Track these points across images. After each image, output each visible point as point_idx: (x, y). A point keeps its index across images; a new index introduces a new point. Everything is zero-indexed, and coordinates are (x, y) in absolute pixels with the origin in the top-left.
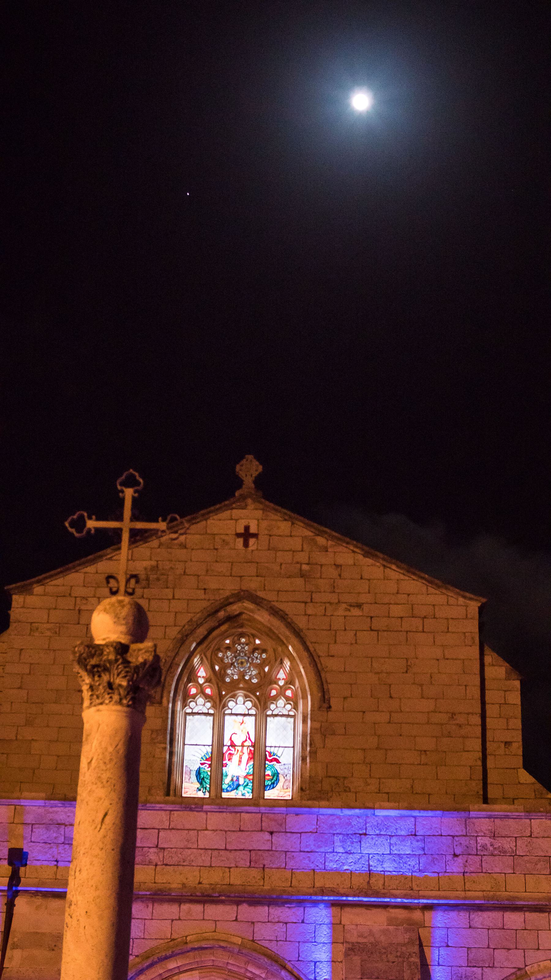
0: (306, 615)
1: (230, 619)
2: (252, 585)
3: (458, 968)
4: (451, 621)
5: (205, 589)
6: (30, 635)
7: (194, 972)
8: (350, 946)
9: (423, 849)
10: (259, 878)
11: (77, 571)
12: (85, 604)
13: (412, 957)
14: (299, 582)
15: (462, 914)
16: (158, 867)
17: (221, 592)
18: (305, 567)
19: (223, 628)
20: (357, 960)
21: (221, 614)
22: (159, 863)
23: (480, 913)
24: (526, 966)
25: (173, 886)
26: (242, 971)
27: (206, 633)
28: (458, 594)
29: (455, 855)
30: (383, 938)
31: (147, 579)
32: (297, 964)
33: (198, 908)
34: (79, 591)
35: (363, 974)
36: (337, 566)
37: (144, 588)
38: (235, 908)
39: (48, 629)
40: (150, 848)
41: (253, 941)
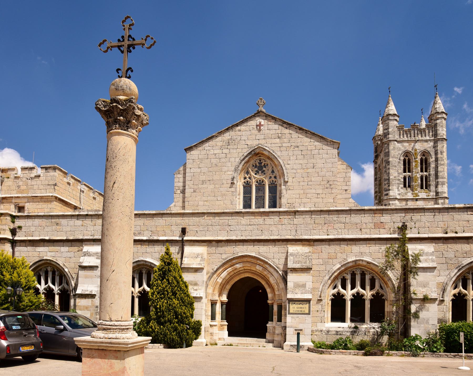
9: (314, 222)
13: (310, 256)
14: (278, 140)
15: (327, 242)
23: (332, 242)
26: (256, 263)
29: (325, 224)
30: (300, 251)
31: (229, 143)
35: (294, 262)
37: (228, 145)
38: (253, 243)
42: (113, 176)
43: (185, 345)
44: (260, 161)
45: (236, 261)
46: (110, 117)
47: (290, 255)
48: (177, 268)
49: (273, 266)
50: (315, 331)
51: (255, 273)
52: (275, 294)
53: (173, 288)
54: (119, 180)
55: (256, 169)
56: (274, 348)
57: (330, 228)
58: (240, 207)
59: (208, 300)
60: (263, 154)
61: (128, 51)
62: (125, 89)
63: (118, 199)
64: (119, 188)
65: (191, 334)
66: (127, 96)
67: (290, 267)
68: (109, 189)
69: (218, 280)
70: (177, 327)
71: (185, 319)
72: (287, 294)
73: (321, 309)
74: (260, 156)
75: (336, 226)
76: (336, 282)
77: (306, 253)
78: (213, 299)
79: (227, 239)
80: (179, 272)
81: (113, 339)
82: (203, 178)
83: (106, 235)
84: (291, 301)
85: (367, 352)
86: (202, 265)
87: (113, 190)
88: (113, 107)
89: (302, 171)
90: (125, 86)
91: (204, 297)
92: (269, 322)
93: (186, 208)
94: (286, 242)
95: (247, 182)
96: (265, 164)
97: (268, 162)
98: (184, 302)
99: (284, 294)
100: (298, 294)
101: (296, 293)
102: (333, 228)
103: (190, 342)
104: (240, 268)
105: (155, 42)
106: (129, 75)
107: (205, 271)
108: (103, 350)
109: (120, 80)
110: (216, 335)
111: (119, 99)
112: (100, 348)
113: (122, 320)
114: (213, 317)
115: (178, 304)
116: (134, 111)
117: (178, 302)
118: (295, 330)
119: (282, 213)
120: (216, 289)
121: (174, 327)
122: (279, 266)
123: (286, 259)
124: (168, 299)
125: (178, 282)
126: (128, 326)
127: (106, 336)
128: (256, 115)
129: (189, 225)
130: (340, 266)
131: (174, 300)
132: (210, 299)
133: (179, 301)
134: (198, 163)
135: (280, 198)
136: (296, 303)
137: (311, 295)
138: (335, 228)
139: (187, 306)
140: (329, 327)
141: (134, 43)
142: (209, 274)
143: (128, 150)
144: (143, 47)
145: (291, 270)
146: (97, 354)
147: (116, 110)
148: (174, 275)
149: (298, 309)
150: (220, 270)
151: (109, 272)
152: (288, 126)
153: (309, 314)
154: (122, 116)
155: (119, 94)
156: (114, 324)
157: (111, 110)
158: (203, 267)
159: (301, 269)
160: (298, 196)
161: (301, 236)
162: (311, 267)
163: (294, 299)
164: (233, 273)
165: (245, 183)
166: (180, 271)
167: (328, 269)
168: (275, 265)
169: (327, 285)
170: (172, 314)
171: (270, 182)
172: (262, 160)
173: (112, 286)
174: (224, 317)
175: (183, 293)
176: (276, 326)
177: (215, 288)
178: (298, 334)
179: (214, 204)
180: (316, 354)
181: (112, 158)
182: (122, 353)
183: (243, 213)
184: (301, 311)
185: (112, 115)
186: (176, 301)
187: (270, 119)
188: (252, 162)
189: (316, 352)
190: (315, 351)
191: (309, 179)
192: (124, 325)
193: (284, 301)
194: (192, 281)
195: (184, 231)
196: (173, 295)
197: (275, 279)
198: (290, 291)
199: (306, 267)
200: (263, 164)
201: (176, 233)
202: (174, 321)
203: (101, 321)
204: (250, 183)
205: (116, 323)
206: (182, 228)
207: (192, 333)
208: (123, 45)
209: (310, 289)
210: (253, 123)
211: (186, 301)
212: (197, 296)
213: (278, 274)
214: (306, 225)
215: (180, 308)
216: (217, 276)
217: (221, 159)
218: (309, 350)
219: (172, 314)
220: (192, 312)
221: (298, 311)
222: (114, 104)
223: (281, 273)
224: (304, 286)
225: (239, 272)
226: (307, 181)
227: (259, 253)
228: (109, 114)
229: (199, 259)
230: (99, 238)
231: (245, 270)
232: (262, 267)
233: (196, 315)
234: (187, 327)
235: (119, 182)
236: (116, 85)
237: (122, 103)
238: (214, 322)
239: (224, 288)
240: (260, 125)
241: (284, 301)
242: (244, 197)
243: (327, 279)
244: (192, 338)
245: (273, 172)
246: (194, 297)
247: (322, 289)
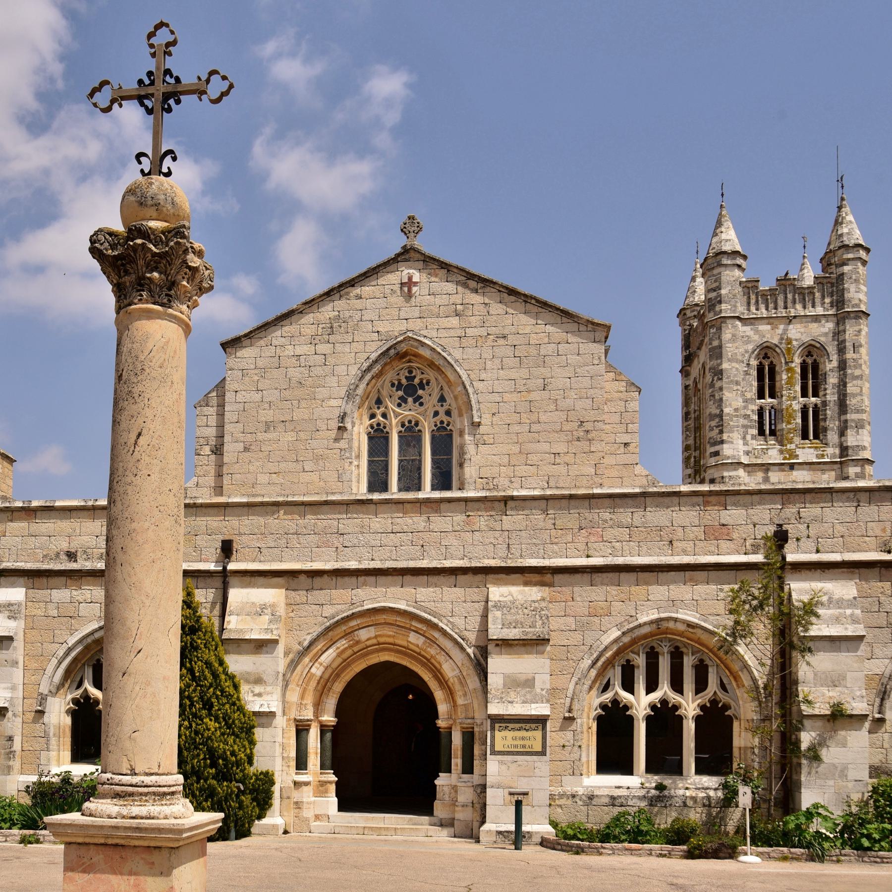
7: (370, 628)
13: (543, 610)
26: (408, 626)
30: (520, 597)
31: (332, 327)
35: (503, 625)
38: (401, 577)
42: (135, 417)
43: (233, 834)
44: (410, 372)
45: (359, 622)
46: (127, 273)
47: (495, 606)
48: (213, 640)
49: (450, 635)
50: (557, 797)
51: (405, 651)
52: (455, 705)
53: (203, 691)
54: (152, 427)
55: (400, 393)
56: (456, 839)
57: (592, 539)
58: (361, 490)
59: (289, 720)
60: (416, 355)
61: (163, 109)
62: (162, 203)
63: (149, 475)
64: (151, 446)
65: (247, 807)
66: (166, 221)
67: (495, 637)
68: (125, 451)
69: (313, 670)
70: (215, 789)
71: (235, 768)
72: (488, 704)
73: (572, 741)
74: (409, 361)
75: (609, 534)
76: (610, 674)
77: (534, 602)
78: (302, 718)
79: (336, 567)
80: (216, 649)
81: (142, 818)
82: (267, 415)
83: (119, 563)
84: (498, 720)
85: (695, 848)
86: (274, 632)
87: (136, 452)
88: (135, 248)
89: (515, 397)
90: (163, 197)
91: (279, 713)
92: (440, 774)
93: (224, 492)
94: (484, 576)
95: (379, 425)
96: (421, 380)
97: (431, 375)
98: (231, 725)
99: (479, 705)
100: (514, 705)
101: (509, 702)
102: (600, 539)
103: (247, 826)
104: (368, 640)
105: (231, 86)
106: (169, 168)
107: (280, 649)
108: (116, 845)
109: (149, 180)
110: (308, 806)
111: (150, 228)
112: (110, 841)
113: (160, 772)
114: (301, 764)
115: (216, 731)
116: (185, 257)
117: (217, 725)
118: (511, 794)
119: (473, 503)
120: (307, 692)
121: (208, 788)
122: (466, 633)
123: (485, 616)
124: (193, 718)
125: (215, 676)
126: (174, 786)
127: (124, 811)
128: (399, 259)
129: (240, 534)
130: (619, 633)
131: (207, 720)
132: (292, 717)
133: (219, 723)
135: (461, 465)
136: (511, 726)
138: (605, 539)
139: (237, 736)
140: (592, 787)
141: (179, 90)
142: (291, 656)
143: (172, 354)
144: (201, 100)
145: (497, 645)
146: (102, 856)
147: (142, 257)
148: (206, 657)
149: (515, 743)
150: (319, 646)
151: (128, 654)
152: (480, 285)
153: (543, 753)
154: (155, 269)
155: (148, 216)
156: (143, 782)
157: (131, 256)
158: (277, 638)
159: (521, 642)
160: (505, 460)
161: (520, 560)
162: (547, 637)
163: (505, 717)
164: (349, 652)
165: (372, 427)
166: (220, 648)
167: (589, 641)
168: (457, 631)
169: (586, 682)
170: (202, 756)
171: (436, 426)
172: (414, 371)
173: (137, 688)
174: (328, 762)
175: (228, 703)
176: (459, 784)
177: (305, 690)
178: (518, 805)
179: (297, 481)
180: (564, 853)
181: (132, 373)
182: (165, 853)
183: (376, 504)
184: (524, 746)
185: (132, 268)
186: (213, 723)
187: (435, 267)
188: (390, 376)
189: (564, 848)
190: (559, 847)
191: (534, 417)
192: (165, 784)
193: (479, 722)
194: (248, 673)
195: (227, 549)
196: (204, 708)
197: (455, 667)
198: (495, 697)
199: (534, 637)
200: (417, 381)
201: (207, 553)
202: (208, 772)
203: (109, 775)
204: (385, 427)
205: (148, 780)
206: (223, 542)
207: (251, 804)
208: (152, 95)
209: (544, 692)
210: (392, 279)
211: (237, 722)
212: (261, 710)
213: (464, 655)
215: (221, 741)
218: (544, 843)
219: (202, 756)
220: (251, 749)
221: (516, 746)
222: (139, 241)
223: (470, 651)
224: (529, 683)
225: (364, 649)
226: (528, 421)
227: (416, 602)
228: (123, 265)
230: (13, 567)
231: (379, 644)
232: (424, 636)
233: (260, 759)
234: (238, 788)
235: (151, 432)
236: (139, 194)
237: (155, 239)
238: (302, 774)
240: (409, 284)
241: (479, 722)
242: (370, 463)
243: (587, 666)
244: (252, 816)
245: (442, 399)
246: (255, 714)
247: (574, 692)
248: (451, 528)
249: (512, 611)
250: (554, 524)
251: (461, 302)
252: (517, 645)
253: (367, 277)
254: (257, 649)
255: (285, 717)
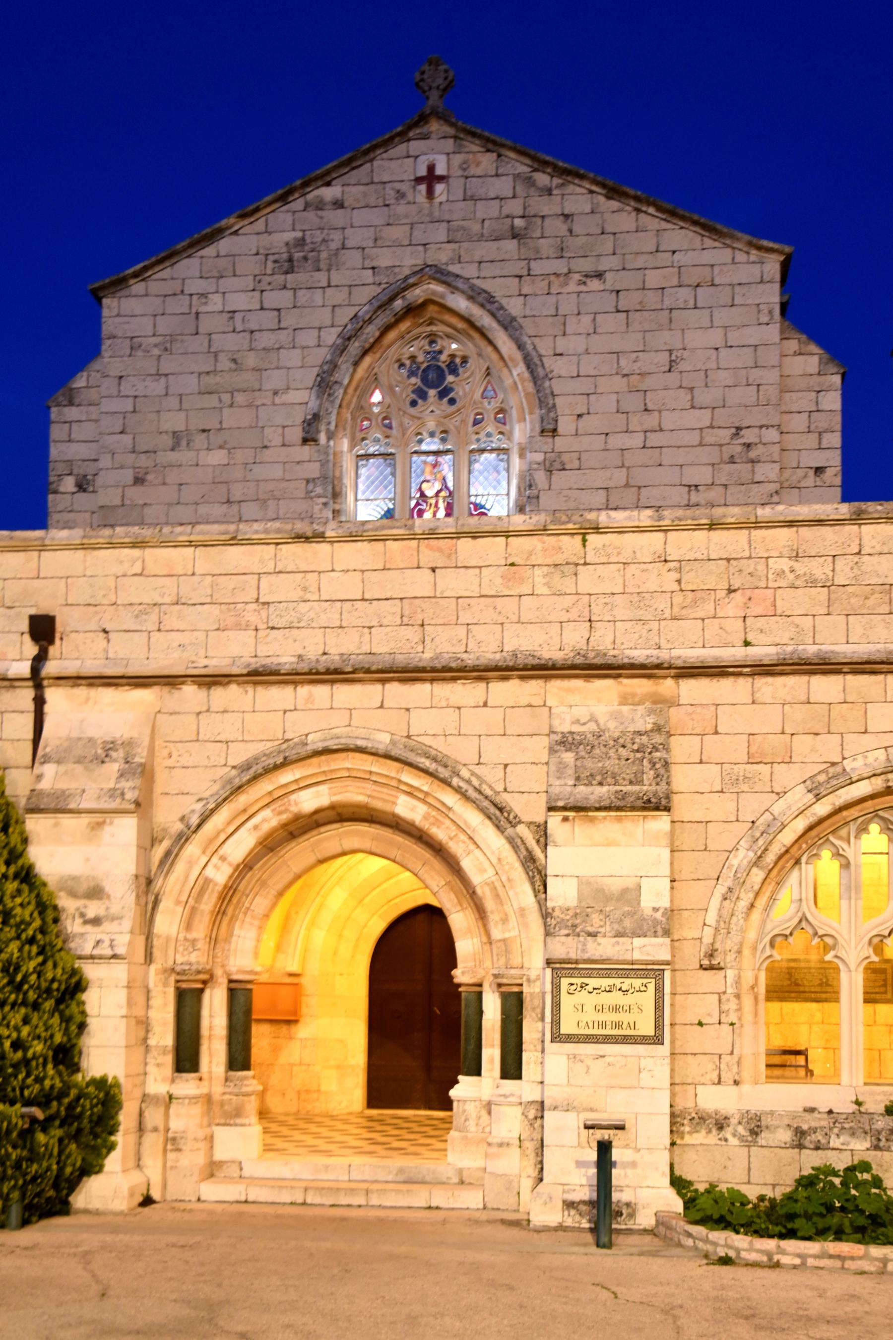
0: (520, 295)
1: (412, 311)
2: (442, 256)
3: (733, 766)
4: (737, 288)
5: (373, 268)
6: (130, 355)
8: (558, 737)
10: (416, 640)
11: (189, 256)
12: (206, 303)
13: (657, 750)
14: (511, 245)
16: (261, 634)
17: (397, 270)
18: (519, 222)
19: (404, 326)
20: (569, 757)
21: (398, 304)
22: (261, 626)
24: (844, 759)
25: (283, 660)
26: (394, 783)
27: (377, 334)
28: (750, 244)
30: (612, 725)
31: (290, 260)
32: (478, 770)
33: (321, 692)
34: (195, 286)
35: (578, 779)
36: (566, 217)
37: (286, 273)
38: (378, 687)
39: (156, 346)
40: (247, 603)
41: (408, 737)
45: (298, 775)
77: (640, 733)
82: (175, 421)
92: (460, 1077)
100: (600, 939)
101: (590, 934)
128: (411, 134)
134: (156, 352)
136: (593, 982)
137: (667, 941)
145: (565, 819)
149: (601, 1017)
152: (556, 181)
153: (657, 1039)
184: (619, 1025)
187: (477, 149)
193: (533, 974)
194: (74, 878)
197: (487, 865)
209: (658, 915)
214: (635, 598)
216: (204, 852)
217: (257, 335)
221: (603, 1025)
229: (114, 767)
232: (424, 802)
239: (245, 914)
240: (431, 178)
243: (745, 862)
248: (477, 589)
249: (597, 751)
250: (679, 581)
251: (521, 214)
252: (605, 818)
253: (353, 169)
254: (93, 829)
255: (153, 968)
